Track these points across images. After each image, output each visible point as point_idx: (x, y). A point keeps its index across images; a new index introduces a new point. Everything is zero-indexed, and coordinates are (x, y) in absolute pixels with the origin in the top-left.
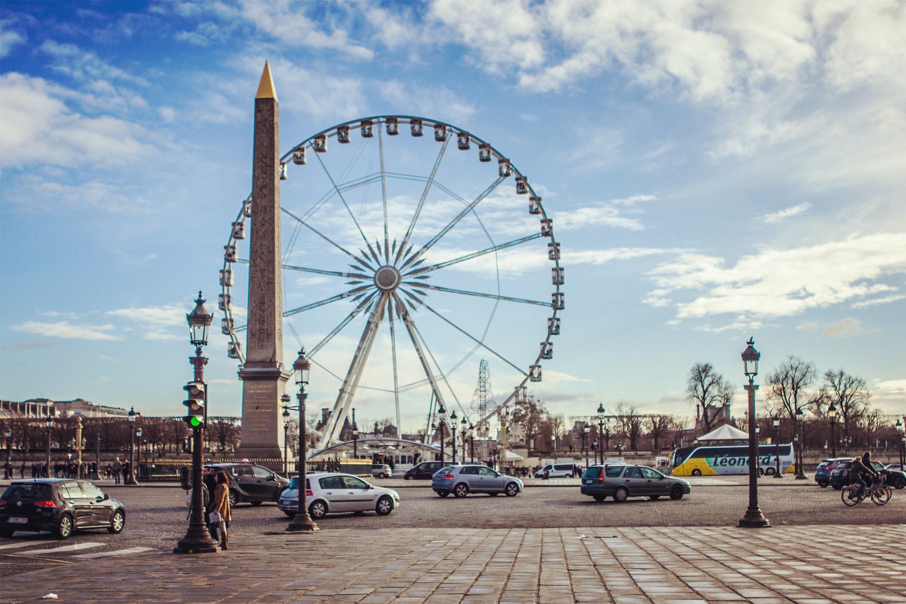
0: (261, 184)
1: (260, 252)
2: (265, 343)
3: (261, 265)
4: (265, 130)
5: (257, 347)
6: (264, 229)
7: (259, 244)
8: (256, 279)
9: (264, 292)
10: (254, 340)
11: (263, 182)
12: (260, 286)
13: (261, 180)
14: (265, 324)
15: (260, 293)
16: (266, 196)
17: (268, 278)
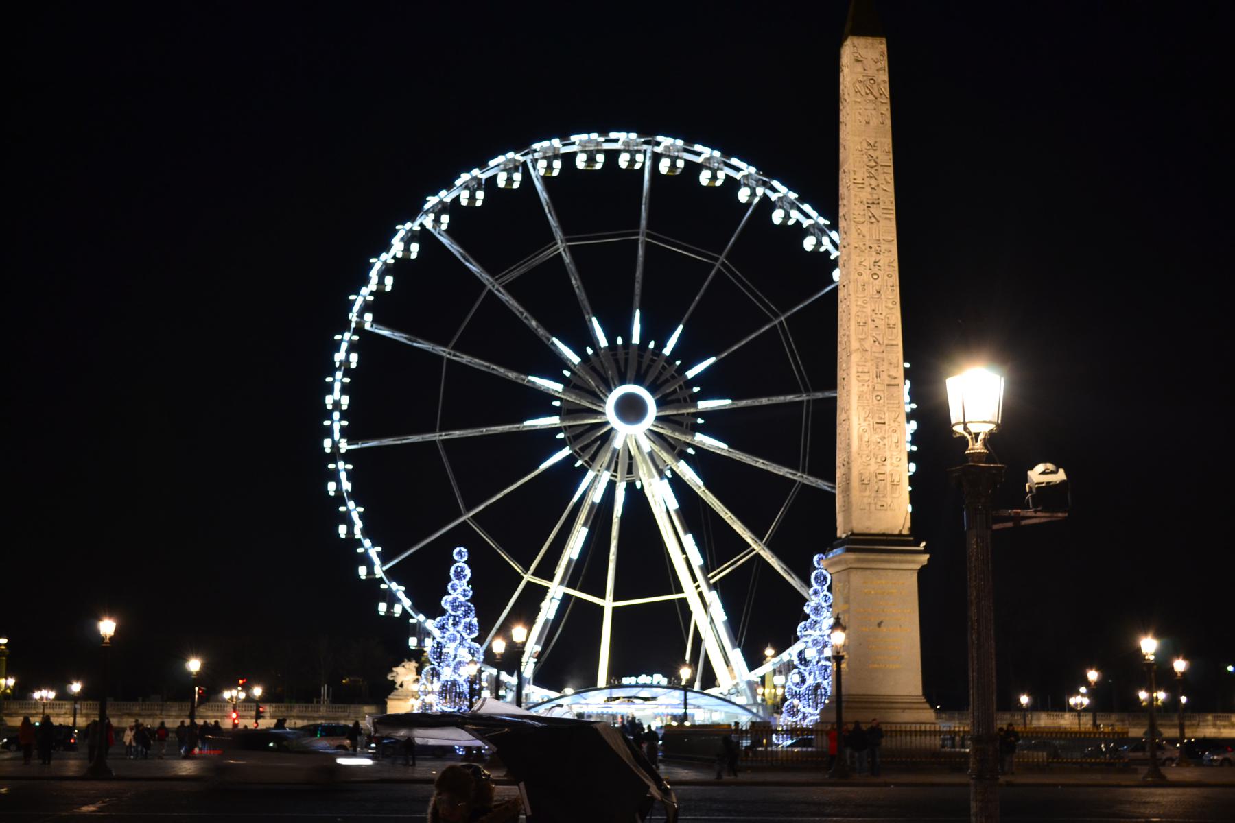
0: (869, 197)
1: (871, 325)
2: (889, 500)
3: (874, 349)
4: (871, 97)
5: (873, 507)
6: (877, 282)
7: (868, 310)
8: (866, 377)
9: (882, 401)
10: (867, 493)
11: (871, 194)
13: (869, 189)
14: (888, 462)
15: (876, 402)
16: (878, 221)
17: (889, 376)
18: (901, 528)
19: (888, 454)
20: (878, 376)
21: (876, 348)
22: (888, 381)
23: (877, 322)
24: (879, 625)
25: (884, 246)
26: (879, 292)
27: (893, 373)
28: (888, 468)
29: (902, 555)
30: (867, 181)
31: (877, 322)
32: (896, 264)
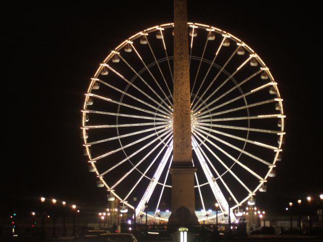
4: (181, 18)
12: (181, 115)
18: (189, 159)
19: (185, 136)
20: (182, 111)
21: (182, 102)
22: (185, 112)
23: (182, 93)
24: (181, 191)
25: (185, 68)
26: (183, 83)
27: (187, 110)
28: (185, 141)
29: (219, 189)
30: (179, 46)
31: (182, 93)
32: (189, 74)
